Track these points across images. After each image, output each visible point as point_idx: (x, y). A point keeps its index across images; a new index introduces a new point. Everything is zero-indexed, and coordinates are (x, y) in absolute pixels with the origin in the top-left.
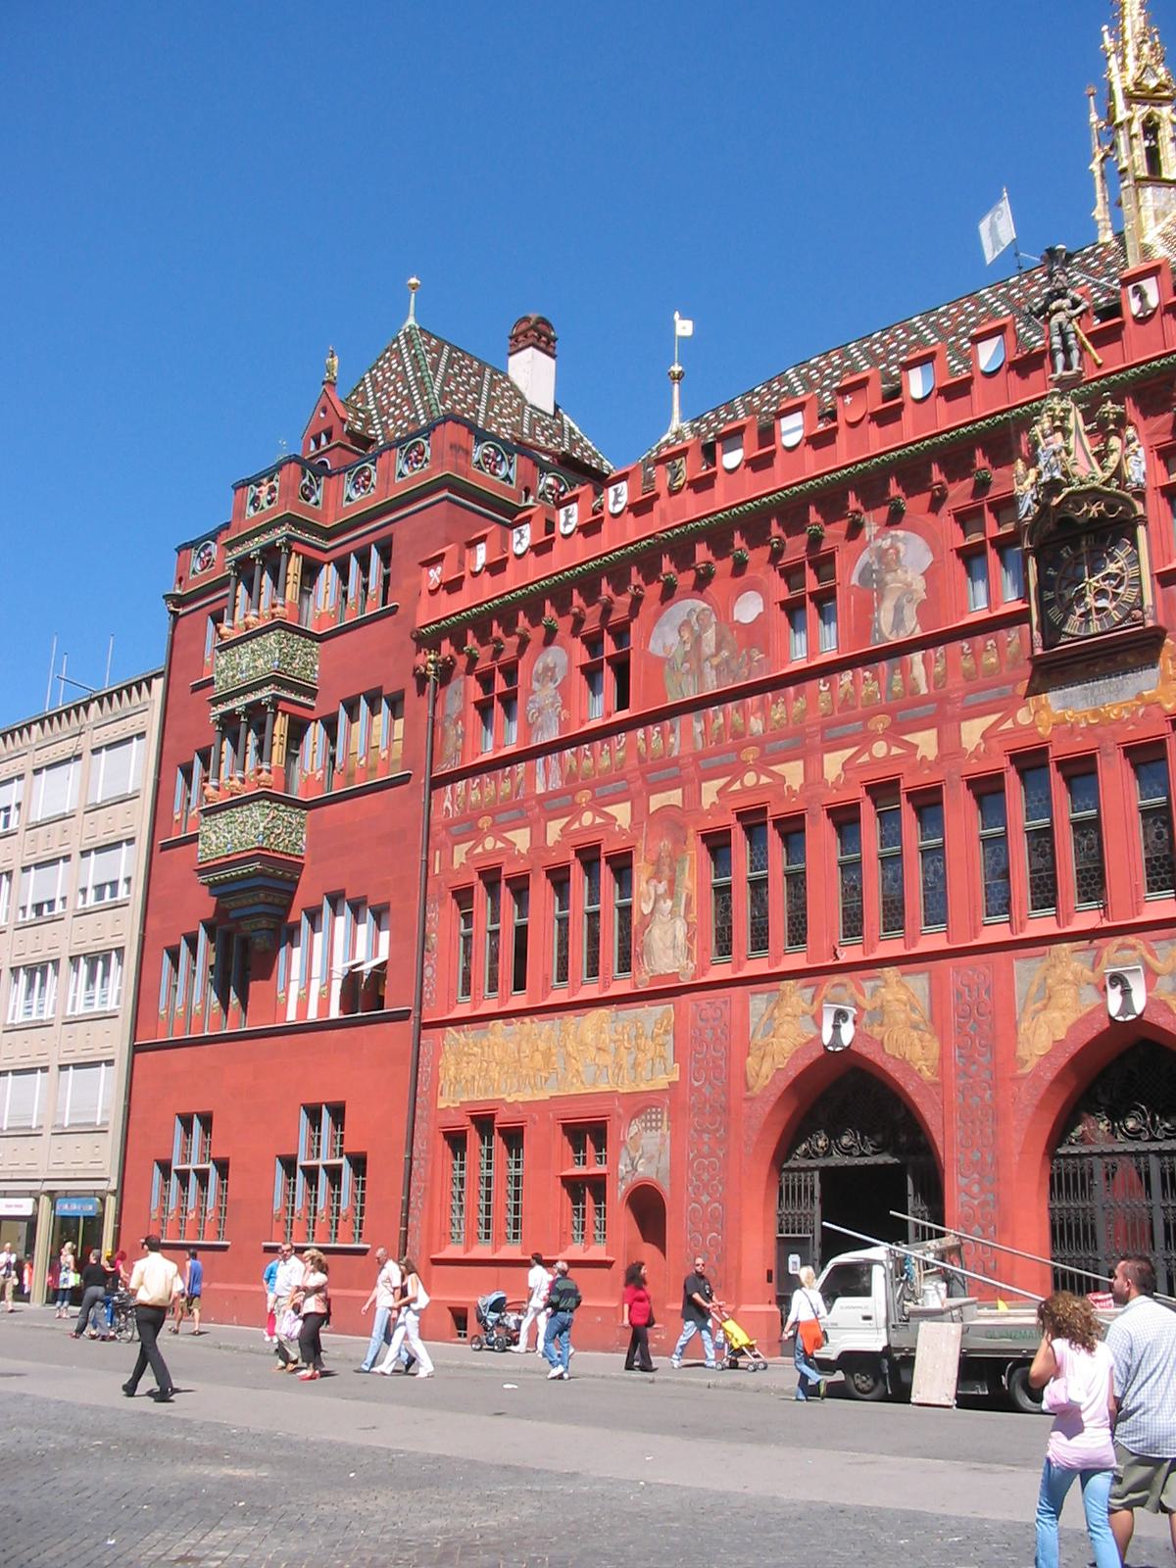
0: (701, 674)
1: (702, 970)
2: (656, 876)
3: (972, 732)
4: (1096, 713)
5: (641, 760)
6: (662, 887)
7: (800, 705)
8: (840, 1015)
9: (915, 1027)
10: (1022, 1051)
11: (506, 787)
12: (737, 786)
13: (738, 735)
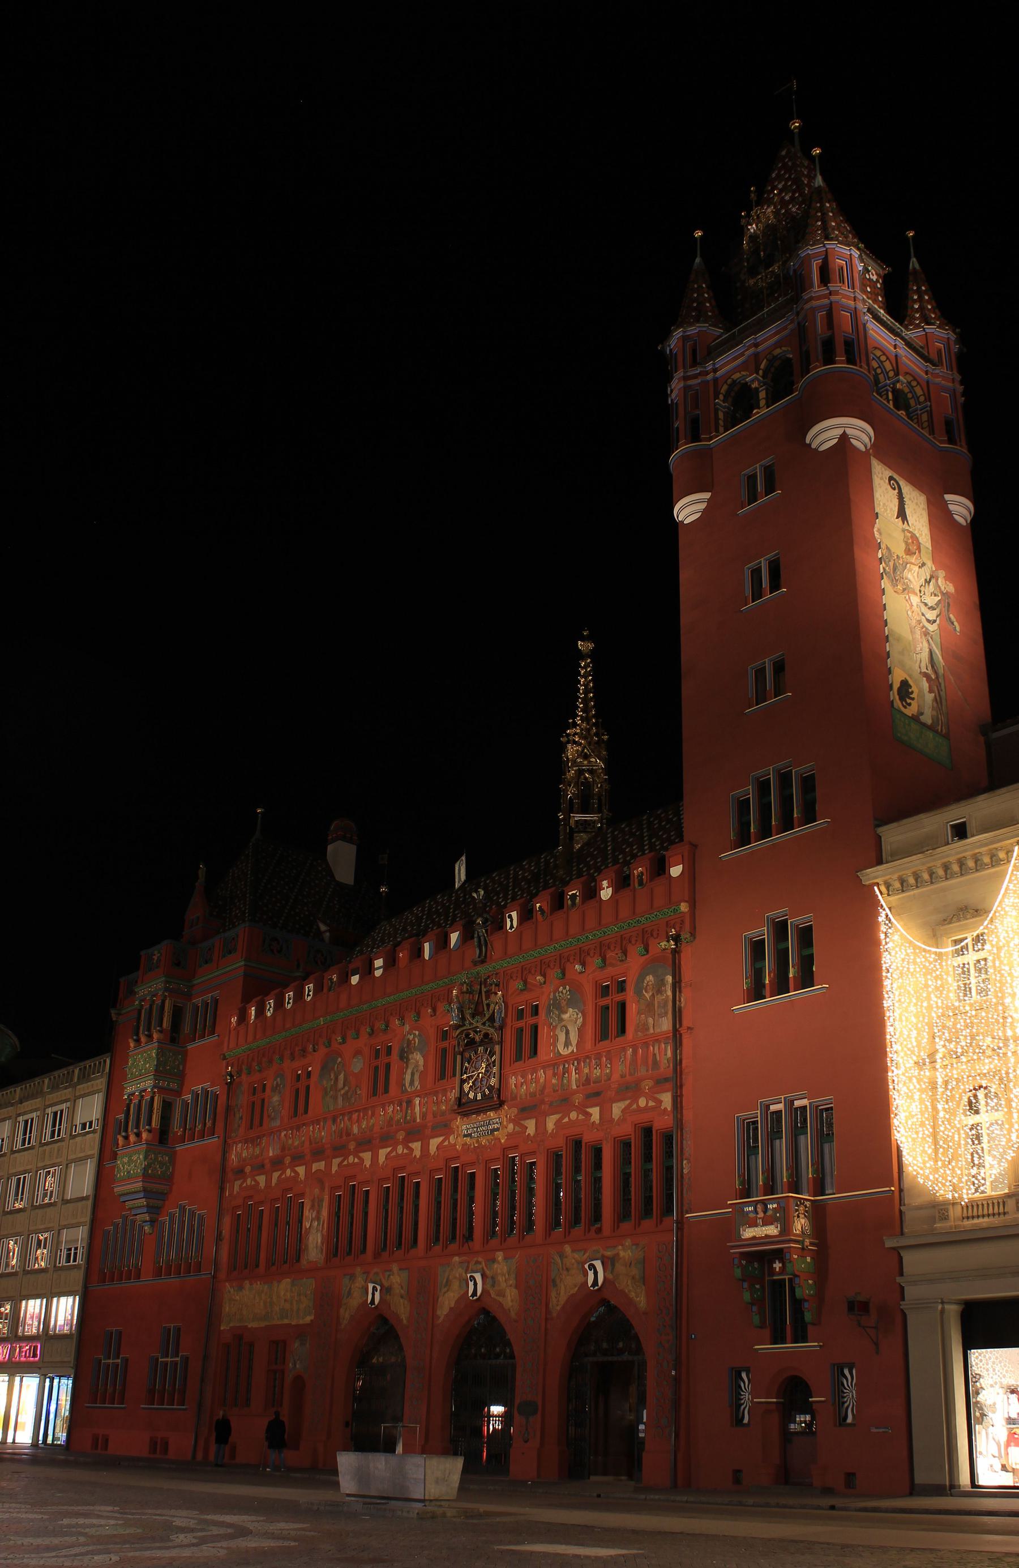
0: (335, 1098)
1: (328, 1259)
2: (312, 1207)
3: (434, 1143)
8: (374, 1289)
9: (402, 1297)
10: (439, 1313)
11: (257, 1151)
12: (345, 1163)
13: (348, 1134)
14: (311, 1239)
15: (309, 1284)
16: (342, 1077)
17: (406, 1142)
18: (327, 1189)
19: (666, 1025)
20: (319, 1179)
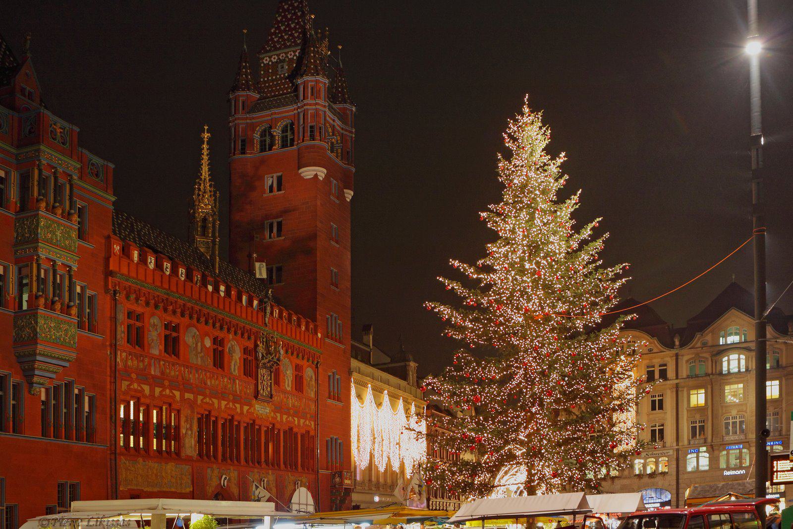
2: (186, 421)
4: (262, 414)
5: (183, 379)
6: (188, 426)
7: (217, 382)
9: (235, 485)
14: (187, 441)
15: (187, 468)
16: (199, 344)
17: (234, 402)
18: (196, 413)
19: (312, 395)
20: (192, 404)
